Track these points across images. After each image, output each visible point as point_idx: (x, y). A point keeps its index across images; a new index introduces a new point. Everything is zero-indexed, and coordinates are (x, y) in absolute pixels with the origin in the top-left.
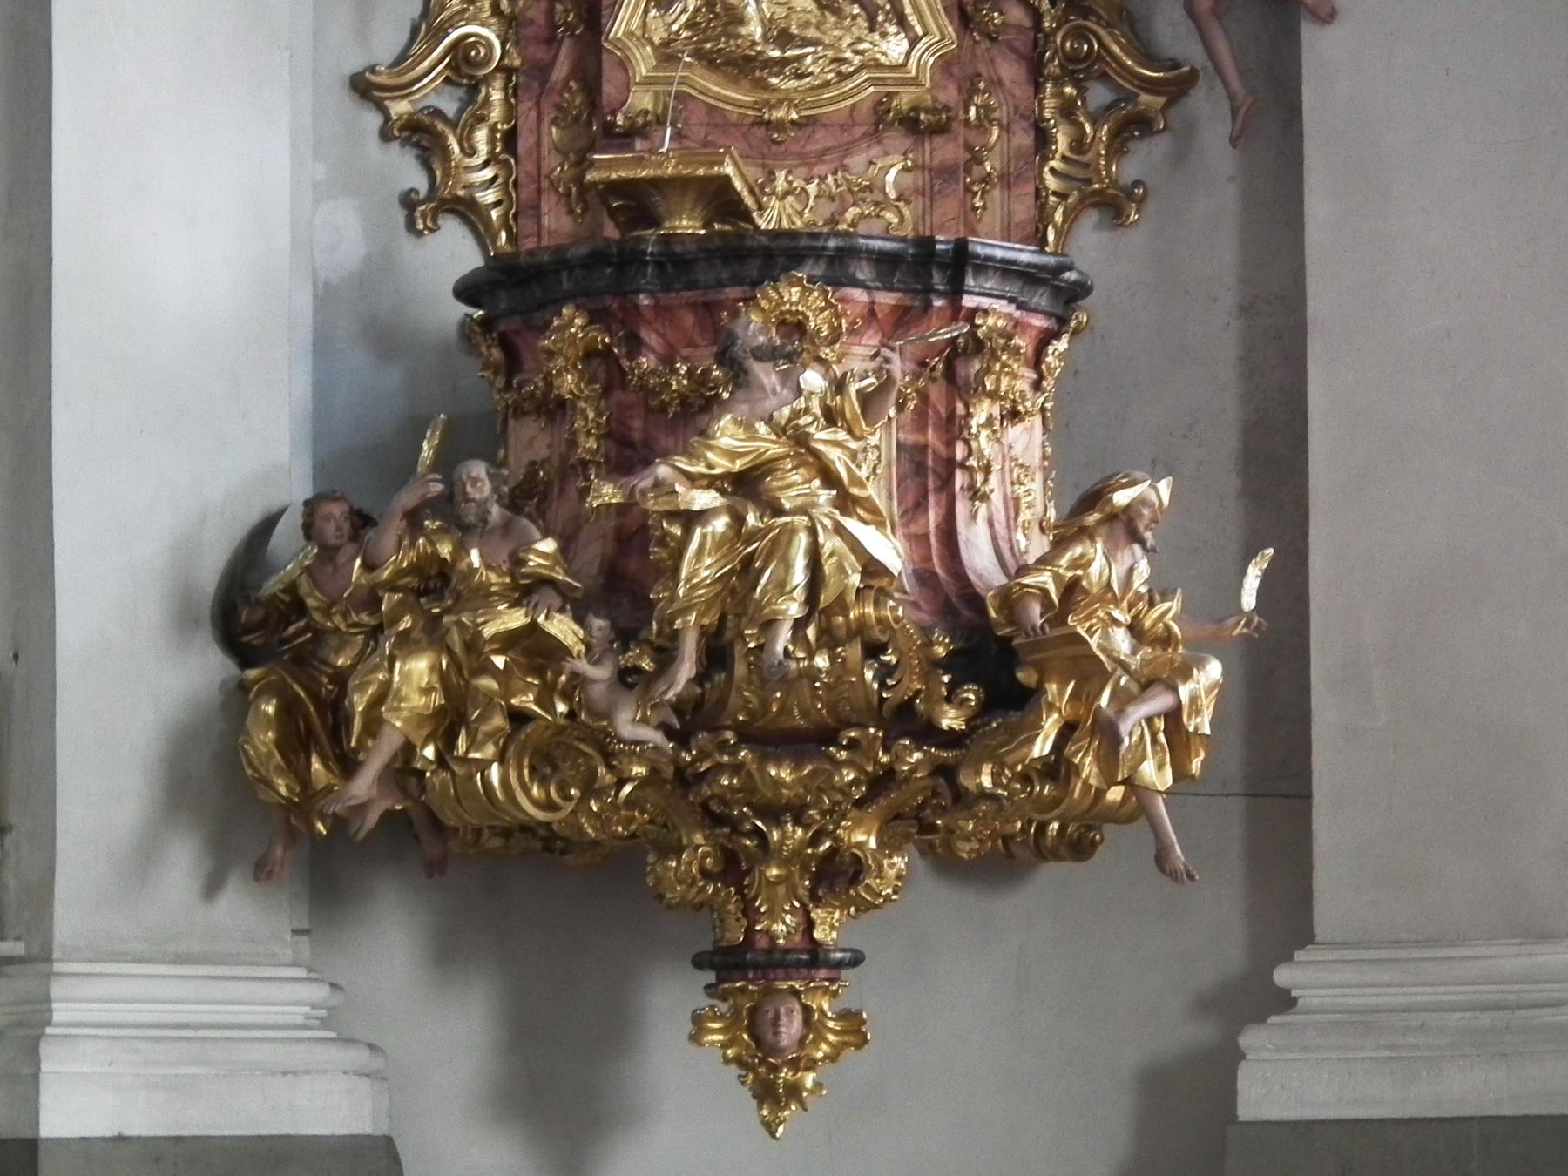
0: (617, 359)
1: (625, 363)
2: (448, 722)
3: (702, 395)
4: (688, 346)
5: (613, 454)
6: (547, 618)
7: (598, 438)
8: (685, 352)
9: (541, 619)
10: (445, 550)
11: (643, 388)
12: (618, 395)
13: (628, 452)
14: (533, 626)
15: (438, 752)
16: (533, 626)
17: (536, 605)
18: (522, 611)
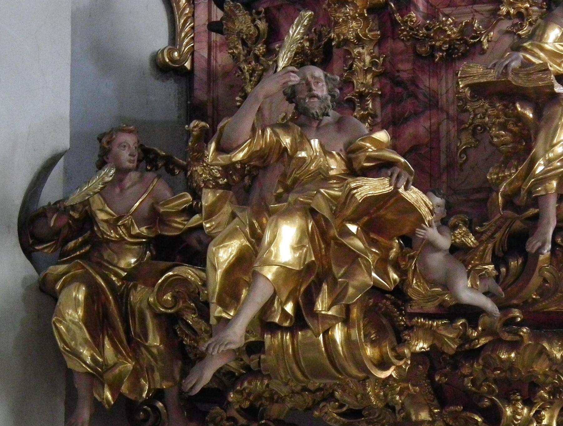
0: (391, 14)
1: (398, 17)
2: (308, 281)
3: (466, 42)
4: (448, 6)
5: (388, 89)
6: (406, 189)
7: (377, 76)
8: (447, 11)
9: (401, 190)
10: (286, 141)
11: (415, 39)
12: (390, 44)
13: (399, 89)
14: (395, 193)
15: (297, 308)
16: (395, 193)
17: (398, 177)
18: (386, 181)
